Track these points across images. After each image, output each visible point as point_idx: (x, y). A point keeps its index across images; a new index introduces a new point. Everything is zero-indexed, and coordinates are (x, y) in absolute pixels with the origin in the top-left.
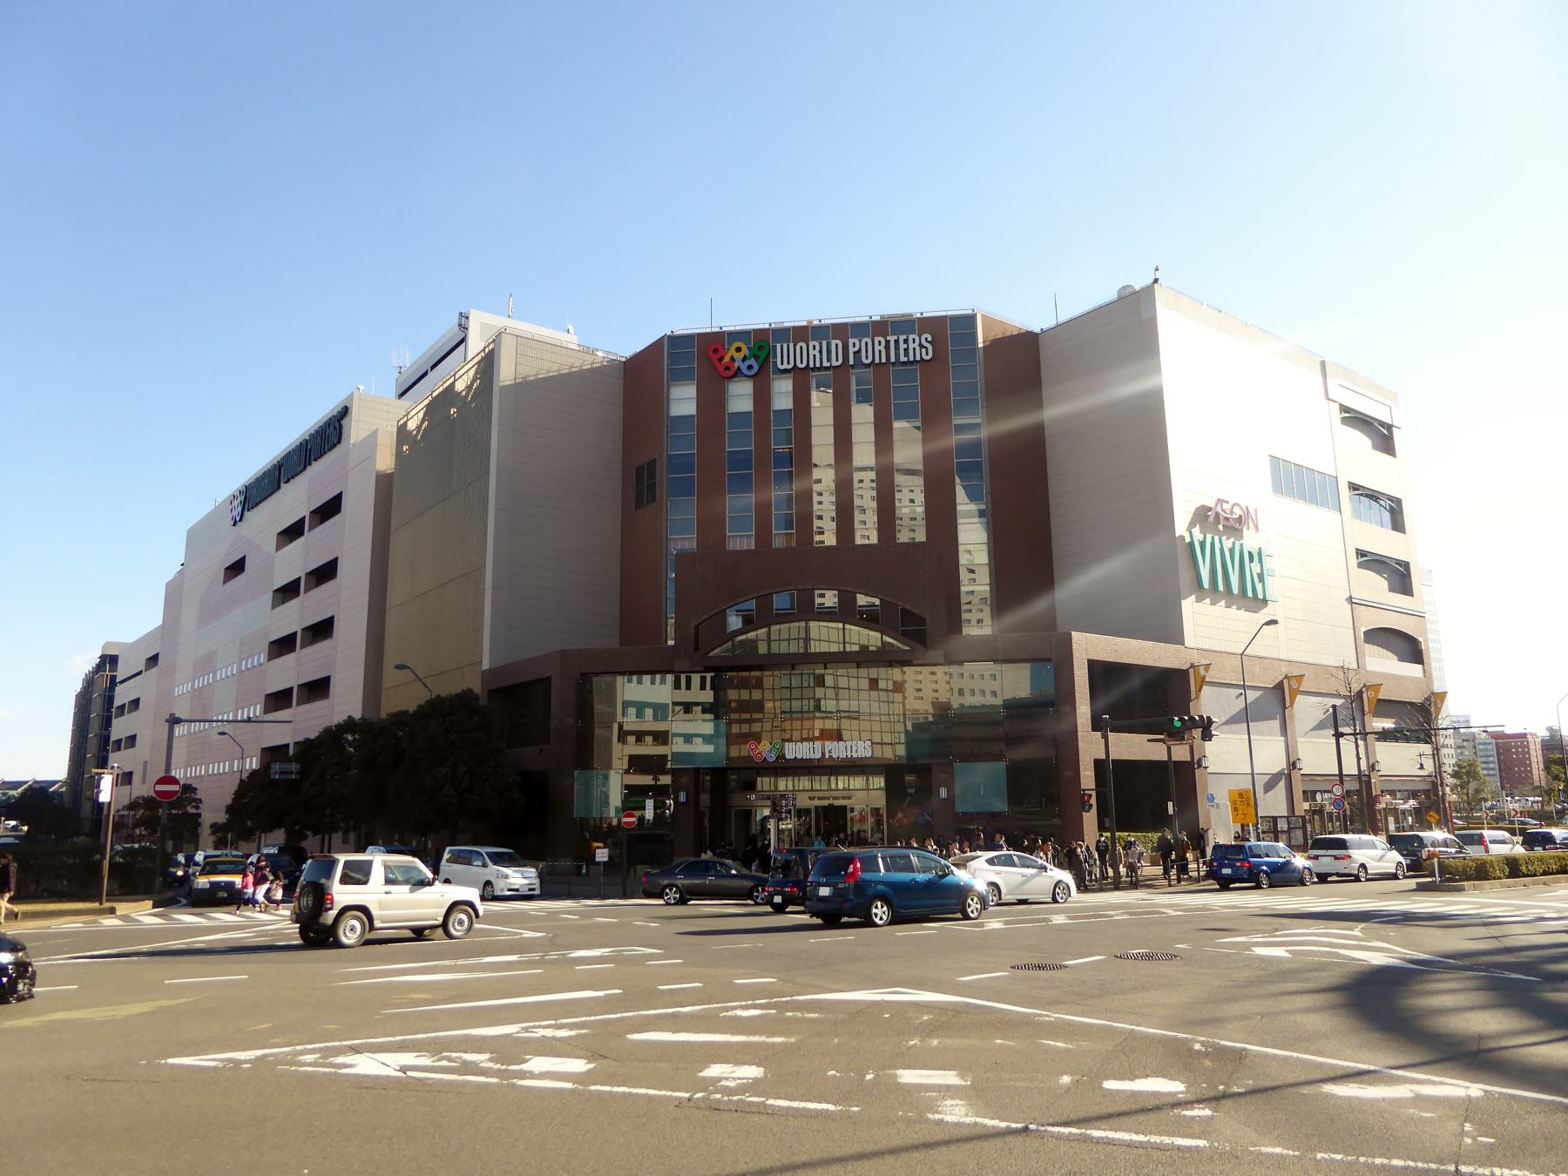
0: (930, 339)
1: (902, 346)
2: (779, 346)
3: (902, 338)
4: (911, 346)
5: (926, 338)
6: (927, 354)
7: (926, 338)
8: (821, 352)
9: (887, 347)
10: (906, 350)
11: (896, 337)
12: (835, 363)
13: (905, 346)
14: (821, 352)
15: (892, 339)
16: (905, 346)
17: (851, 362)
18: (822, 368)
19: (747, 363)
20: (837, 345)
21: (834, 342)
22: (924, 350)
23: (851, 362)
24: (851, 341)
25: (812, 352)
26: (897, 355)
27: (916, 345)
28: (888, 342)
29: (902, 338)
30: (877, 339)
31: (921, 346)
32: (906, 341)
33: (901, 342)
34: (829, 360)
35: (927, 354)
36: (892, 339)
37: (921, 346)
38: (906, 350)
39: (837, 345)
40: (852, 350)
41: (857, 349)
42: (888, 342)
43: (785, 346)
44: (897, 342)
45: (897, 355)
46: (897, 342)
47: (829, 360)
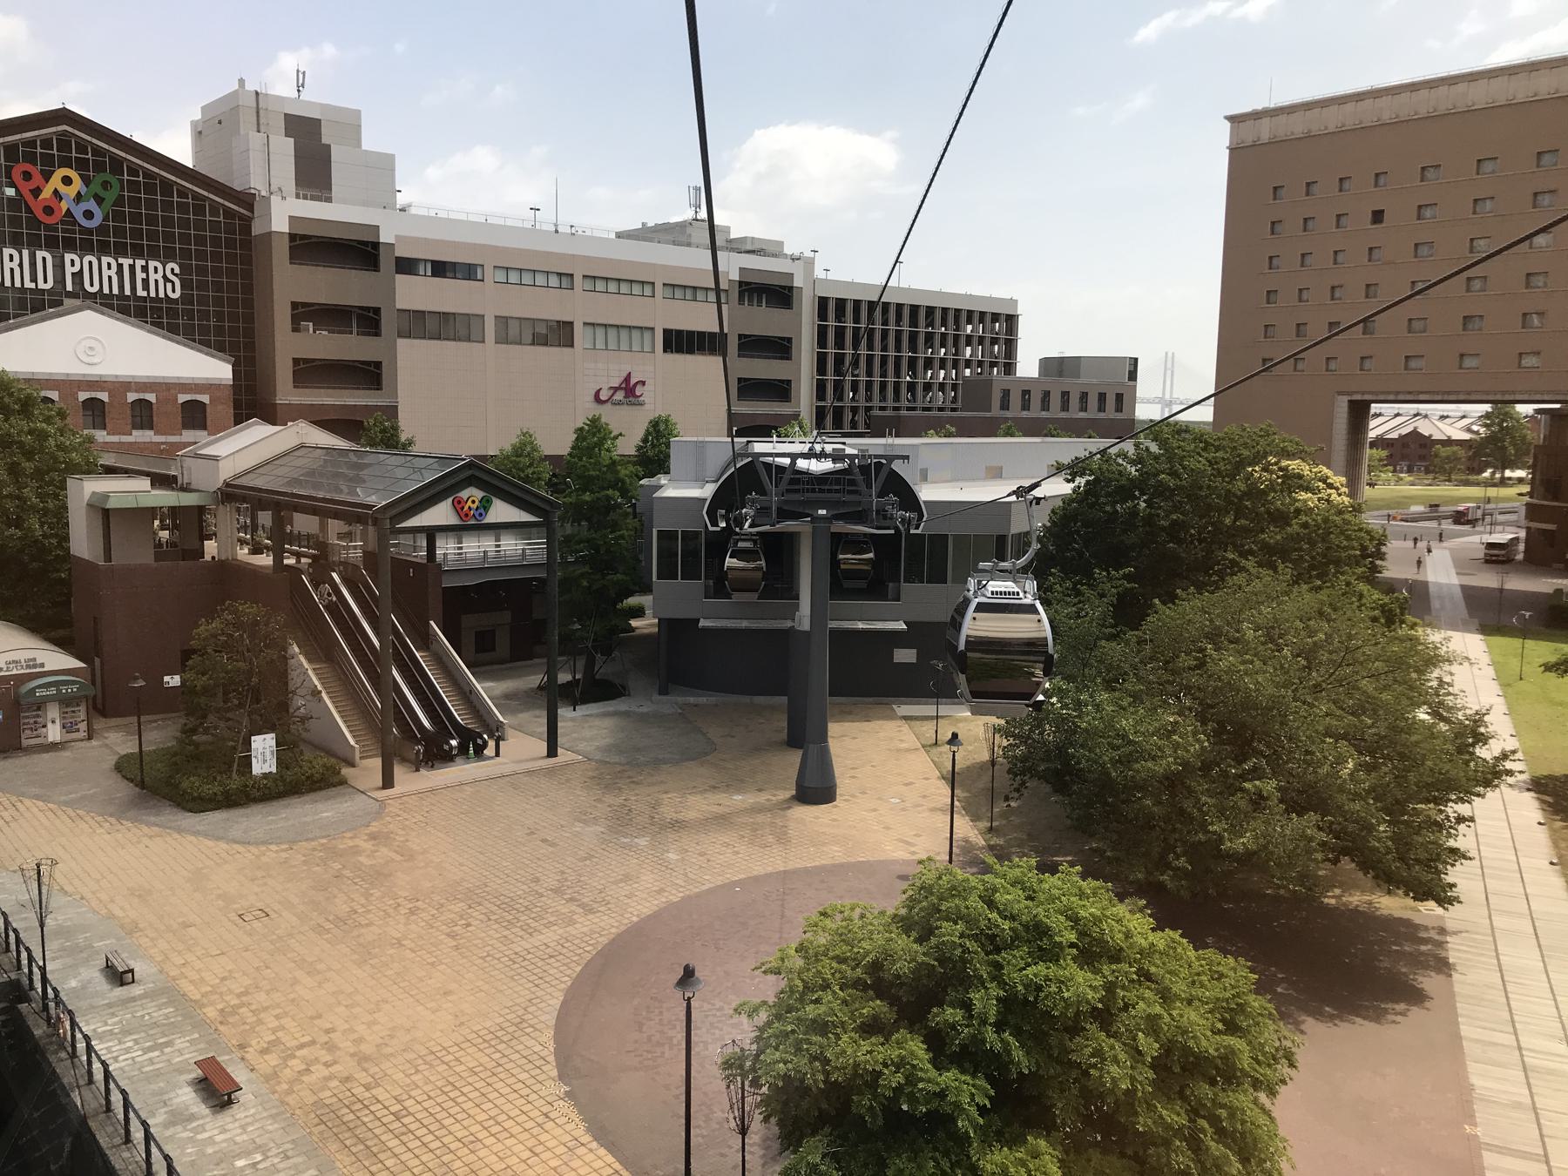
0: (177, 270)
1: (140, 275)
5: (172, 270)
6: (174, 291)
7: (172, 270)
8: (21, 265)
10: (146, 282)
11: (131, 262)
12: (41, 285)
13: (144, 275)
14: (21, 265)
15: (126, 262)
16: (144, 275)
17: (69, 288)
18: (23, 289)
19: (479, 511)
20: (44, 259)
21: (40, 254)
22: (169, 286)
23: (69, 288)
24: (68, 257)
26: (133, 288)
27: (159, 276)
28: (120, 266)
29: (140, 263)
30: (105, 260)
31: (165, 277)
32: (145, 269)
34: (34, 279)
35: (174, 291)
39: (44, 259)
40: (69, 270)
41: (76, 269)
42: (120, 266)
44: (132, 267)
45: (133, 288)
46: (132, 267)
47: (34, 279)
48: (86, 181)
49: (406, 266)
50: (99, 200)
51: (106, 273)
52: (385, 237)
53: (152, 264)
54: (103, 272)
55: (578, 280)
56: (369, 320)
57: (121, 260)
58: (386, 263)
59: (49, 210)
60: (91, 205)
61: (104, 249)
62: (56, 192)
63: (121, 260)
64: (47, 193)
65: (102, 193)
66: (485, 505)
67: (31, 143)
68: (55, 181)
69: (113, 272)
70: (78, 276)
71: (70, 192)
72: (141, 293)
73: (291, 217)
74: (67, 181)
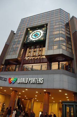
1: (38, 80)
3: (38, 79)
4: (39, 80)
9: (35, 80)
10: (38, 81)
28: (35, 79)
31: (41, 80)
32: (39, 79)
34: (25, 82)
36: (36, 79)
37: (41, 80)
38: (38, 81)
42: (35, 79)
44: (37, 79)
46: (37, 79)
47: (25, 82)
51: (33, 80)
68: (11, 79)
69: (34, 80)
70: (30, 81)
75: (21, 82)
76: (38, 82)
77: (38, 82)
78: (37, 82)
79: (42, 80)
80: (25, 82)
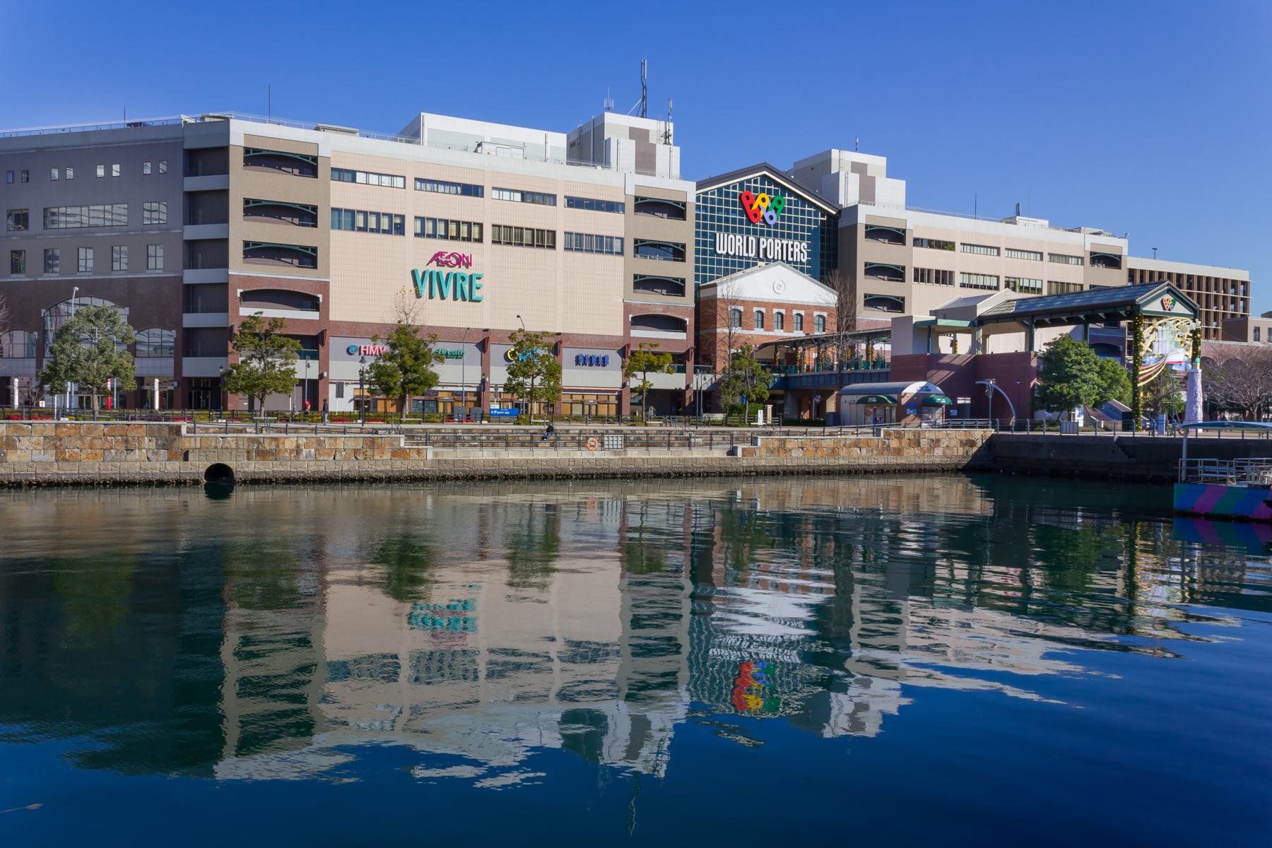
1: (790, 249)
2: (718, 235)
3: (791, 243)
9: (782, 248)
10: (792, 253)
12: (751, 255)
15: (785, 242)
17: (761, 256)
24: (762, 239)
25: (738, 244)
27: (798, 250)
28: (782, 244)
29: (791, 243)
30: (777, 241)
31: (801, 252)
32: (792, 246)
33: (790, 246)
34: (747, 252)
37: (801, 252)
38: (792, 253)
40: (762, 247)
41: (764, 246)
42: (782, 244)
43: (722, 235)
44: (787, 245)
46: (787, 245)
47: (747, 252)
48: (772, 200)
49: (918, 242)
50: (776, 210)
52: (909, 227)
53: (796, 243)
54: (773, 245)
55: (1003, 251)
56: (896, 273)
57: (783, 242)
58: (909, 240)
59: (756, 216)
60: (772, 212)
61: (776, 235)
62: (759, 206)
63: (783, 242)
64: (755, 207)
65: (777, 206)
66: (1174, 303)
67: (728, 187)
68: (759, 201)
69: (779, 248)
71: (764, 206)
72: (790, 259)
73: (867, 215)
74: (764, 200)
75: (730, 252)
76: (792, 256)
77: (792, 256)
78: (790, 259)
79: (803, 250)
80: (746, 255)
